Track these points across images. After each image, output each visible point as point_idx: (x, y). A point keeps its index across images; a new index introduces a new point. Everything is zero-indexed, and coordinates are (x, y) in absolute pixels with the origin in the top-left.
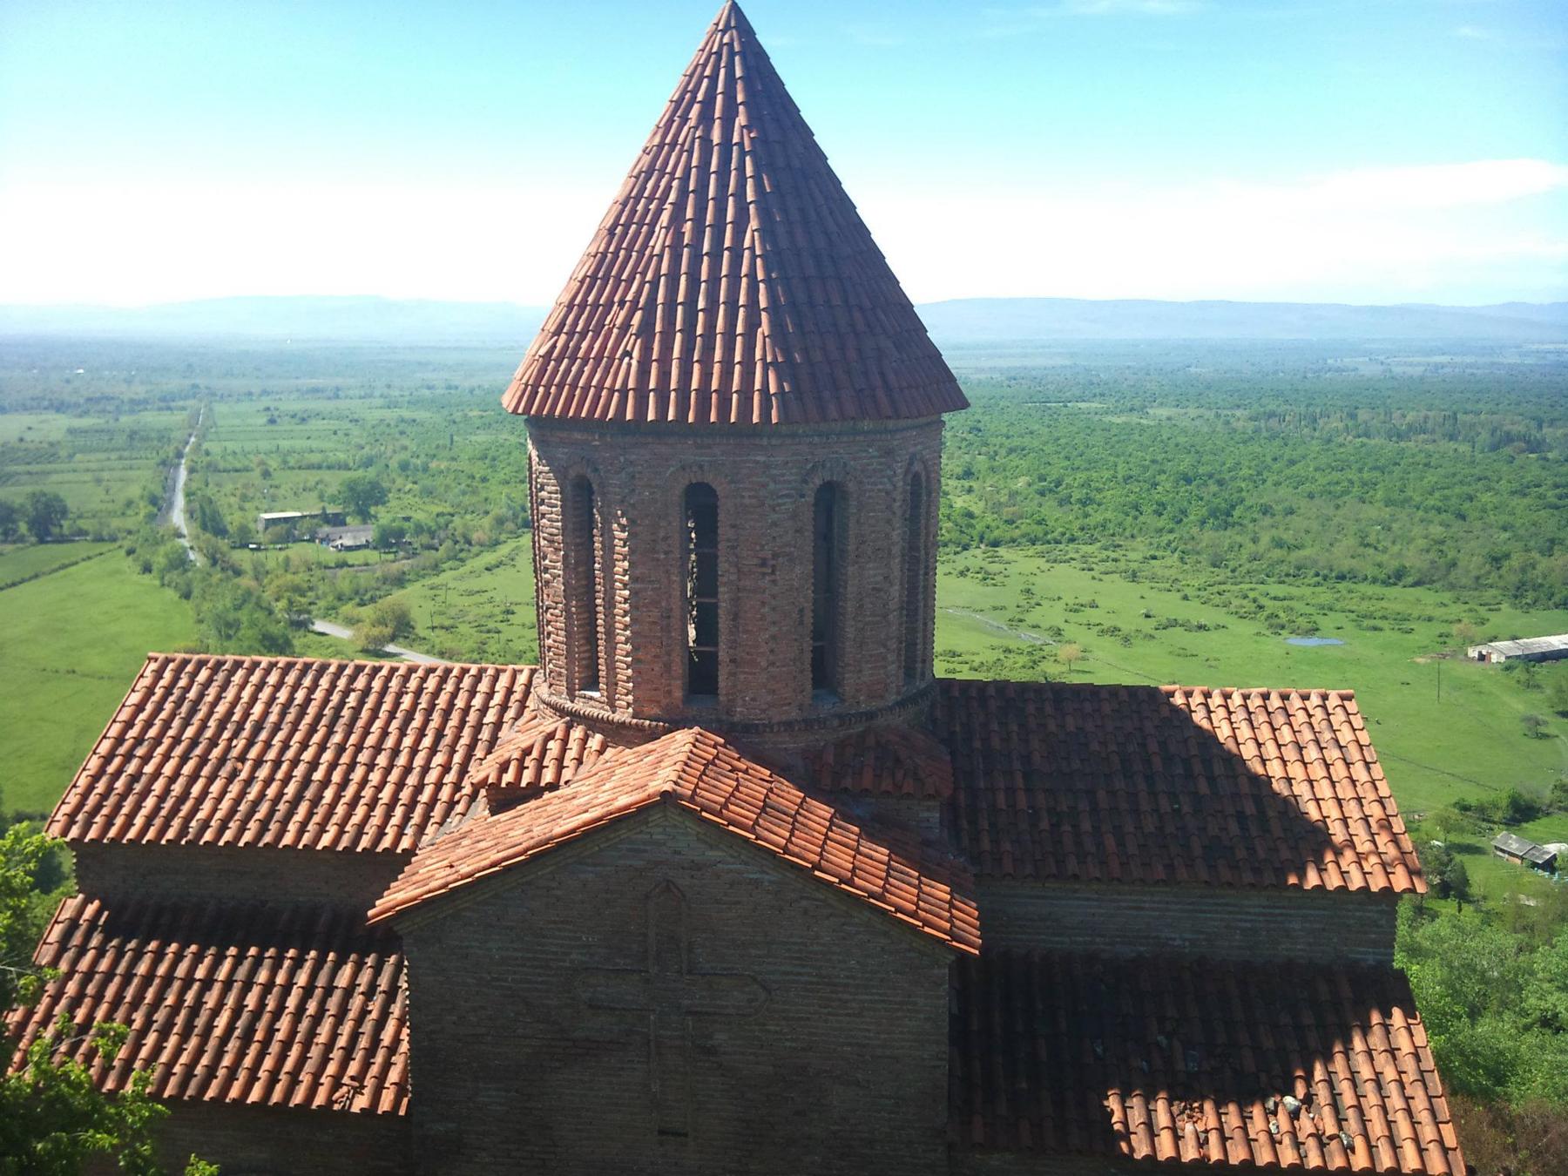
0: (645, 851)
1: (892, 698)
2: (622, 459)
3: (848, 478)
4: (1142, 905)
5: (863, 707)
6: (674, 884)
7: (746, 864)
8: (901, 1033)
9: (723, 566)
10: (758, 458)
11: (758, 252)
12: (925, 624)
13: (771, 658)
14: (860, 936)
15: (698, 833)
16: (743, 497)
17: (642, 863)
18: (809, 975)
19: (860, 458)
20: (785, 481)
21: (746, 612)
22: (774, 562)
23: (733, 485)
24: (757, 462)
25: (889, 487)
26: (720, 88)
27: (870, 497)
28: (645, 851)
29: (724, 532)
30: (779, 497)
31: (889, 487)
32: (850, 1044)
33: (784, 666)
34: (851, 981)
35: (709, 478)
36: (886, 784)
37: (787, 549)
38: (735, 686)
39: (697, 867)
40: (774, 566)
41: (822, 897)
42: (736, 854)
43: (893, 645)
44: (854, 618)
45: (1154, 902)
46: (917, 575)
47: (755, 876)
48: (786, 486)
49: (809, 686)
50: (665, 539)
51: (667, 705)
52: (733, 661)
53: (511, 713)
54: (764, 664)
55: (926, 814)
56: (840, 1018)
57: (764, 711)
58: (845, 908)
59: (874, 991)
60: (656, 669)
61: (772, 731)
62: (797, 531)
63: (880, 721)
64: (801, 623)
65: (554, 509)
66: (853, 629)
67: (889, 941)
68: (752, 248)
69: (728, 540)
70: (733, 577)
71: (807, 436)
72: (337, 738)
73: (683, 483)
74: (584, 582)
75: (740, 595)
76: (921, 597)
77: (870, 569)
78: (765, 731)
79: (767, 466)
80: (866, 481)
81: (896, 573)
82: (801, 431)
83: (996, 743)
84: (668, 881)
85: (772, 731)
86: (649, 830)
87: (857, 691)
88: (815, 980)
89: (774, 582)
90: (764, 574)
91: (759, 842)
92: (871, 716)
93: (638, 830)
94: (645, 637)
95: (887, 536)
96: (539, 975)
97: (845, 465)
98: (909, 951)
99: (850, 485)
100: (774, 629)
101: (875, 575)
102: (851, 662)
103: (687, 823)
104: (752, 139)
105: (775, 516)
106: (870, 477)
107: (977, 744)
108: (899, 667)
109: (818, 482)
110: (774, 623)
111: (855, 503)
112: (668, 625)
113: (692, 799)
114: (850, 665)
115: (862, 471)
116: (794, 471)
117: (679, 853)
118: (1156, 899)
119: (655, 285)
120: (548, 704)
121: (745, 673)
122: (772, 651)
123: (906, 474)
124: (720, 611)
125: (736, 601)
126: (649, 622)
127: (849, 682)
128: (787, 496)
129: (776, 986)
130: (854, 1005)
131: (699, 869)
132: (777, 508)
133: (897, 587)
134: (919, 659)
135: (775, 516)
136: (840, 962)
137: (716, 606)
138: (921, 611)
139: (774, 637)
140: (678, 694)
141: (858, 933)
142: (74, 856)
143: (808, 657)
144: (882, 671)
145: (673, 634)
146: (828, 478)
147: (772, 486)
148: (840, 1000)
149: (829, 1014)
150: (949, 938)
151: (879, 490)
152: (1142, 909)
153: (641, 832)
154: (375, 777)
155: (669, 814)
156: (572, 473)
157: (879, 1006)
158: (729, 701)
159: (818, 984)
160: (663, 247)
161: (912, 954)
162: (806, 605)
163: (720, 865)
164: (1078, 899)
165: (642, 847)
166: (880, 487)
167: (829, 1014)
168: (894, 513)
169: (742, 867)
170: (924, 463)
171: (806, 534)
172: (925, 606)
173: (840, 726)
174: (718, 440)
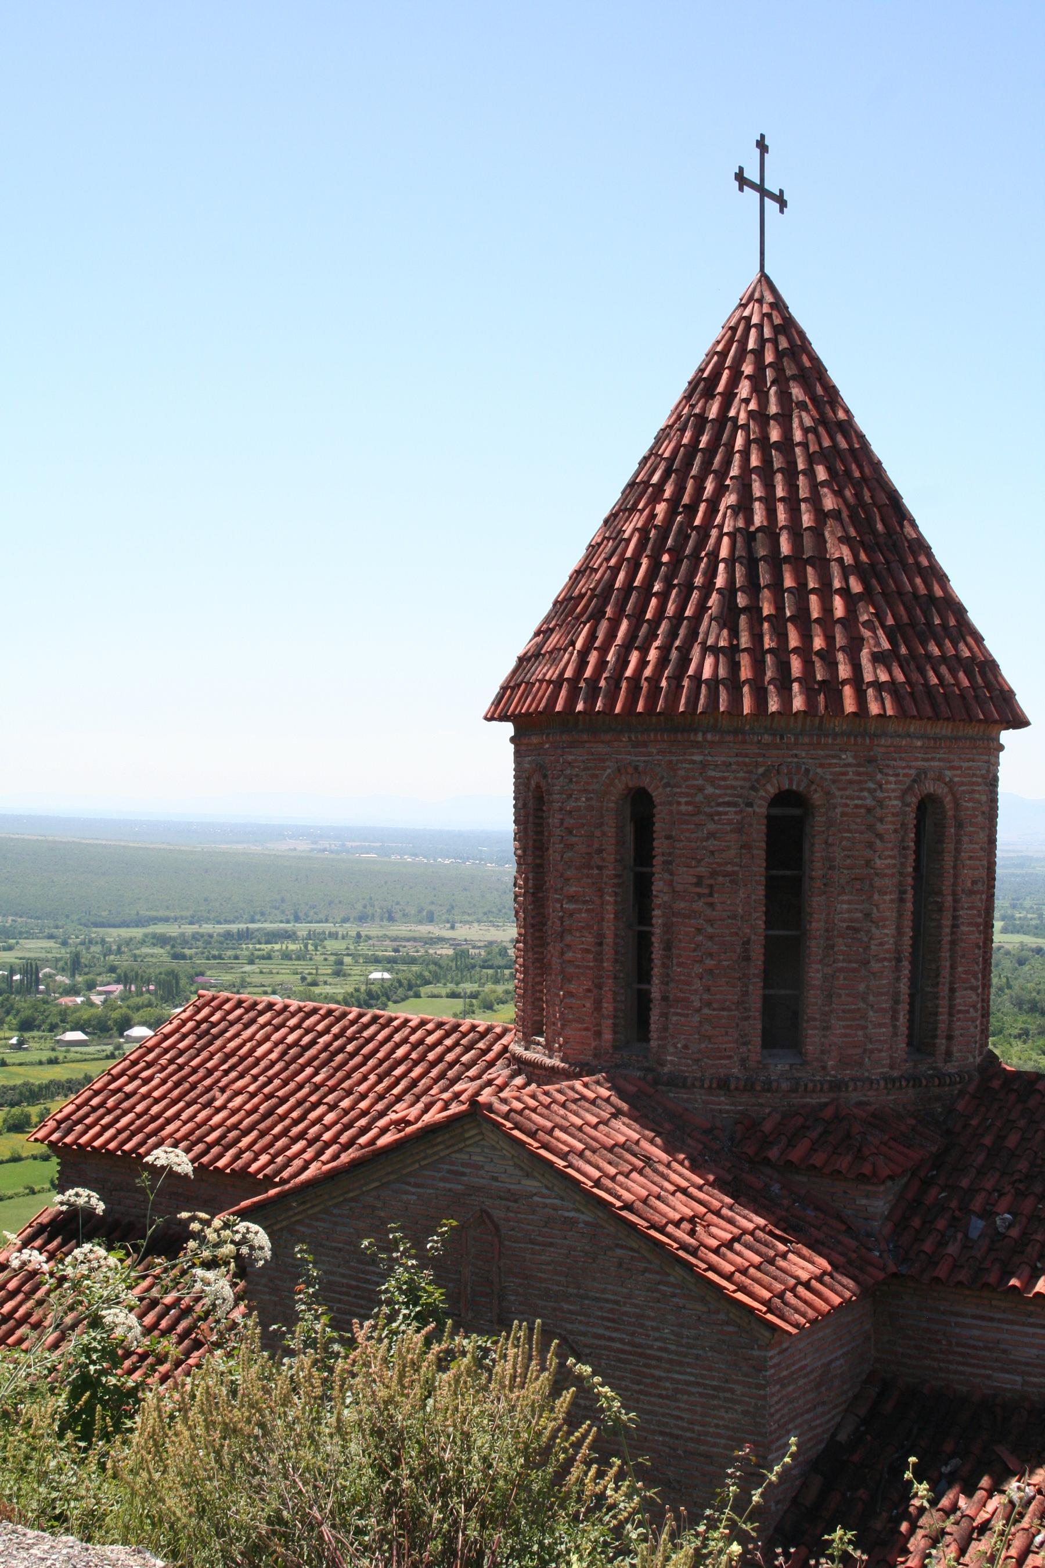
0: (463, 1174)
3: (813, 787)
6: (489, 1216)
7: (562, 1199)
8: (717, 1426)
9: (658, 886)
10: (694, 758)
11: (725, 530)
12: (952, 990)
13: (706, 996)
14: (675, 1300)
15: (513, 1156)
16: (679, 803)
17: (460, 1187)
18: (622, 1341)
19: (830, 764)
20: (727, 787)
21: (680, 941)
22: (711, 882)
23: (669, 789)
24: (694, 762)
25: (869, 802)
26: (727, 364)
27: (843, 814)
28: (463, 1174)
29: (660, 845)
30: (719, 805)
32: (662, 1433)
33: (723, 1009)
34: (664, 1355)
35: (646, 782)
36: (818, 1159)
37: (729, 868)
38: (665, 1029)
39: (513, 1197)
40: (711, 886)
41: (635, 1246)
42: (550, 1185)
44: (820, 962)
47: (572, 1214)
48: (729, 791)
49: (759, 1040)
50: (600, 851)
51: (595, 1048)
52: (665, 998)
53: (395, 1023)
54: (697, 1004)
55: (864, 1202)
56: (653, 1399)
57: (697, 1061)
59: (689, 1370)
60: (588, 1005)
61: (702, 1087)
62: (742, 847)
64: (747, 959)
66: (819, 975)
67: (705, 1309)
68: (721, 527)
69: (663, 855)
70: (666, 898)
71: (754, 734)
72: (317, 1079)
73: (620, 786)
75: (675, 920)
77: (843, 902)
78: (693, 1085)
79: (704, 765)
80: (838, 793)
82: (747, 727)
83: (1012, 1140)
84: (482, 1211)
85: (702, 1087)
86: (468, 1149)
87: (823, 1052)
88: (627, 1348)
89: (711, 905)
90: (700, 895)
91: (569, 1171)
92: (837, 1086)
93: (456, 1148)
94: (578, 967)
95: (868, 863)
97: (807, 771)
98: (728, 1323)
99: (816, 796)
100: (709, 962)
102: (817, 1016)
104: (751, 414)
105: (712, 826)
106: (845, 789)
107: (987, 1140)
108: (895, 1034)
109: (772, 790)
110: (711, 955)
111: (824, 819)
112: (600, 953)
113: (506, 1116)
114: (815, 1019)
115: (834, 782)
116: (741, 774)
117: (496, 1179)
119: (615, 571)
121: (678, 1014)
122: (708, 990)
123: (905, 792)
125: (668, 927)
126: (581, 949)
127: (813, 1039)
128: (729, 804)
129: (588, 1351)
130: (668, 1384)
131: (516, 1201)
132: (716, 818)
133: (891, 930)
135: (712, 826)
136: (654, 1329)
138: (946, 973)
139: (710, 971)
140: (608, 1036)
141: (674, 1295)
142: (58, 1164)
143: (755, 1002)
144: (860, 1033)
145: (605, 964)
147: (710, 790)
148: (653, 1376)
149: (640, 1392)
150: (764, 1309)
151: (857, 806)
153: (460, 1151)
154: (329, 1118)
155: (484, 1131)
156: (533, 783)
157: (694, 1390)
159: (630, 1353)
160: (635, 529)
161: (730, 1329)
163: (536, 1198)
164: (1031, 1325)
166: (859, 802)
167: (640, 1392)
168: (880, 837)
169: (557, 1202)
170: (950, 785)
171: (755, 852)
172: (953, 967)
174: (652, 735)
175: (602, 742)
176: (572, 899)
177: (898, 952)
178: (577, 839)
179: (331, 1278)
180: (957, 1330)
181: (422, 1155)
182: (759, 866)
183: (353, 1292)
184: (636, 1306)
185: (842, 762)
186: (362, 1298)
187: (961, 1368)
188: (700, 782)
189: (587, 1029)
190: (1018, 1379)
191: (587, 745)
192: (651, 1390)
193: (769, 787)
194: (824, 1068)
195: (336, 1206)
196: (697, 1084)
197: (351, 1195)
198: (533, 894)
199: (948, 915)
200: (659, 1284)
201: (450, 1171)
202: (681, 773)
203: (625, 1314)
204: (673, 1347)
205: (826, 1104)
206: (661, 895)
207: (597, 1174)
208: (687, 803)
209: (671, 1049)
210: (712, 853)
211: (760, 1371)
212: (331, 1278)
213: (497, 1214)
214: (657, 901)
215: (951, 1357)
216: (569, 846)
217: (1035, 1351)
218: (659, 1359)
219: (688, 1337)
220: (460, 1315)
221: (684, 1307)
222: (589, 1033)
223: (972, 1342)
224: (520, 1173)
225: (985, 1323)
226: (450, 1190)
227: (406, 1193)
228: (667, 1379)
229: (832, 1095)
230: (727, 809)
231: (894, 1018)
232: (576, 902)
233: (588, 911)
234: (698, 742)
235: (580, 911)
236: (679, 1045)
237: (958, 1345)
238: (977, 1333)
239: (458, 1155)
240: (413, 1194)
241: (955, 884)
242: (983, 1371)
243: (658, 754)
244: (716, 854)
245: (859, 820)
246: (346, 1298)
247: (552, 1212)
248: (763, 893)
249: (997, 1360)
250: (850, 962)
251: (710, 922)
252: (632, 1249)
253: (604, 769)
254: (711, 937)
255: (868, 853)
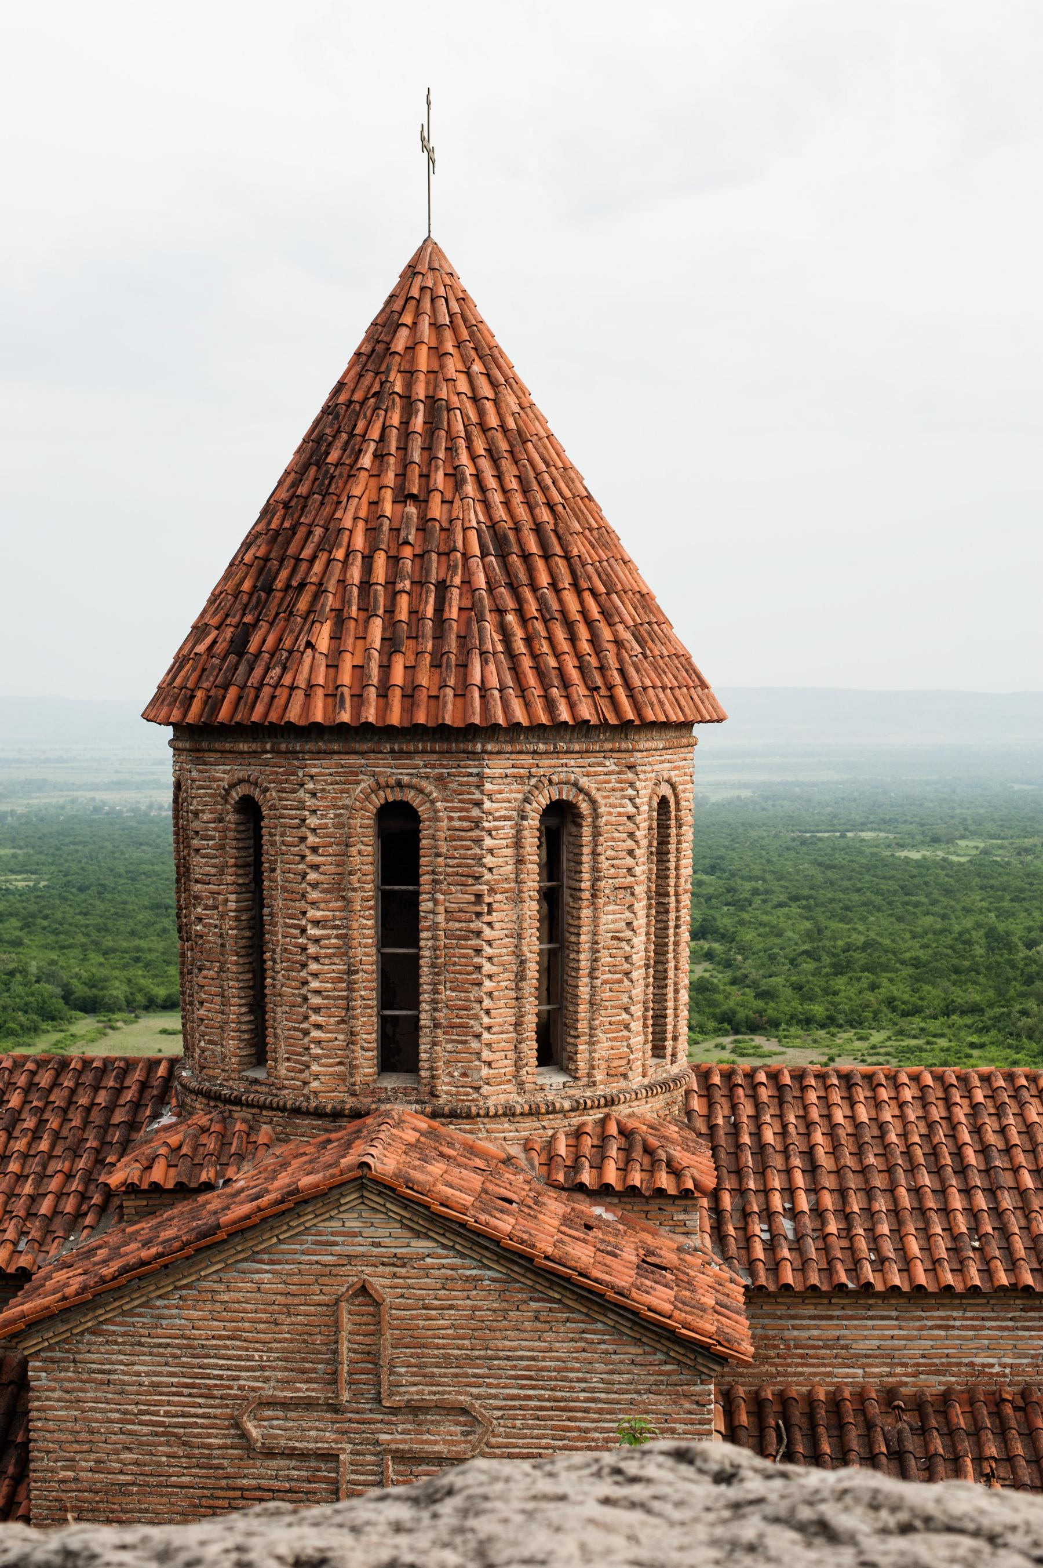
0: (336, 1244)
1: (636, 1080)
2: (300, 774)
4: (952, 1323)
5: (601, 1090)
7: (463, 1256)
13: (486, 1020)
16: (451, 819)
17: (330, 1258)
18: (540, 1398)
19: (596, 774)
25: (631, 809)
28: (336, 1244)
30: (496, 819)
31: (631, 809)
34: (592, 1405)
35: (410, 796)
39: (400, 1261)
40: (489, 905)
43: (637, 1010)
45: (967, 1319)
46: (667, 928)
47: (474, 1272)
58: (585, 1310)
63: (621, 1111)
65: (211, 843)
67: (640, 1351)
69: (434, 873)
73: (377, 801)
74: (248, 934)
76: (671, 956)
78: (478, 1115)
81: (641, 922)
86: (341, 1216)
89: (490, 924)
90: (479, 915)
92: (611, 1102)
93: (327, 1216)
94: (327, 998)
96: (200, 1406)
98: (666, 1363)
101: (614, 922)
103: (388, 1205)
106: (608, 797)
109: (544, 801)
110: (490, 977)
118: (969, 1314)
120: (198, 1093)
121: (453, 1041)
124: (422, 962)
130: (596, 1435)
131: (403, 1266)
134: (669, 1036)
136: (579, 1380)
137: (417, 957)
138: (671, 974)
141: (603, 1342)
146: (556, 797)
148: (579, 1429)
151: (620, 814)
152: (953, 1327)
156: (235, 795)
158: (433, 1077)
159: (552, 1409)
161: (668, 1367)
162: (529, 955)
163: (429, 1260)
164: (871, 1318)
165: (333, 1238)
166: (621, 810)
169: (458, 1261)
173: (573, 1110)
175: (355, 753)
176: (316, 923)
177: (648, 958)
178: (323, 859)
179: (154, 1379)
180: (796, 1333)
181: (285, 1228)
182: (532, 881)
183: (186, 1391)
184: (558, 1359)
185: (605, 769)
186: (201, 1396)
187: (800, 1369)
188: (477, 796)
189: (340, 1063)
190: (860, 1371)
191: (335, 757)
192: (578, 1444)
193: (541, 798)
194: (594, 1084)
195: (160, 1297)
196: (482, 1112)
197: (184, 1282)
198: (237, 919)
199: (672, 915)
200: (583, 1332)
201: (316, 1243)
202: (454, 786)
203: (548, 1369)
204: (603, 1396)
205: (603, 1122)
206: (431, 916)
207: (509, 1228)
208: (460, 819)
209: (447, 1079)
210: (490, 870)
211: (704, 1405)
212: (154, 1379)
213: (377, 1283)
214: (424, 924)
215: (789, 1360)
216: (315, 867)
217: (876, 1343)
218: (586, 1411)
219: (620, 1383)
220: (337, 1398)
221: (615, 1353)
222: (342, 1068)
223: (811, 1342)
224: (409, 1234)
225: (824, 1322)
226: (317, 1263)
227: (258, 1272)
228: (595, 1430)
229: (606, 1110)
230: (503, 823)
231: (645, 1026)
232: (324, 928)
233: (337, 937)
234: (474, 753)
235: (329, 937)
236: (456, 1074)
237: (796, 1347)
238: (816, 1333)
239: (327, 1224)
240: (267, 1272)
241: (676, 886)
242: (822, 1369)
243: (425, 766)
244: (495, 871)
245: (621, 828)
246: (177, 1398)
247: (450, 1272)
248: (537, 907)
249: (836, 1357)
250: (615, 973)
251: (489, 943)
252: (552, 1300)
253: (358, 783)
254: (490, 959)
255: (629, 861)
